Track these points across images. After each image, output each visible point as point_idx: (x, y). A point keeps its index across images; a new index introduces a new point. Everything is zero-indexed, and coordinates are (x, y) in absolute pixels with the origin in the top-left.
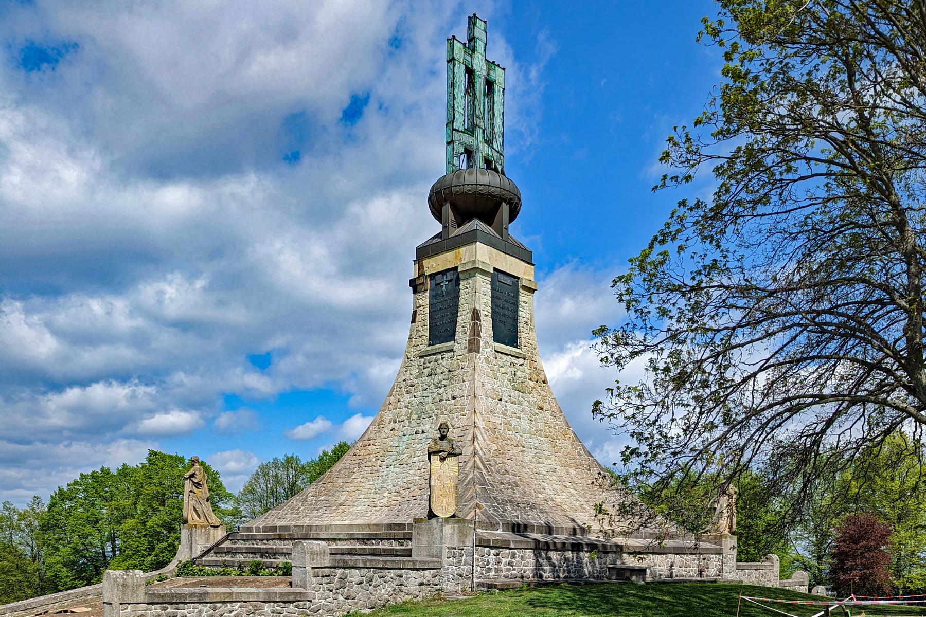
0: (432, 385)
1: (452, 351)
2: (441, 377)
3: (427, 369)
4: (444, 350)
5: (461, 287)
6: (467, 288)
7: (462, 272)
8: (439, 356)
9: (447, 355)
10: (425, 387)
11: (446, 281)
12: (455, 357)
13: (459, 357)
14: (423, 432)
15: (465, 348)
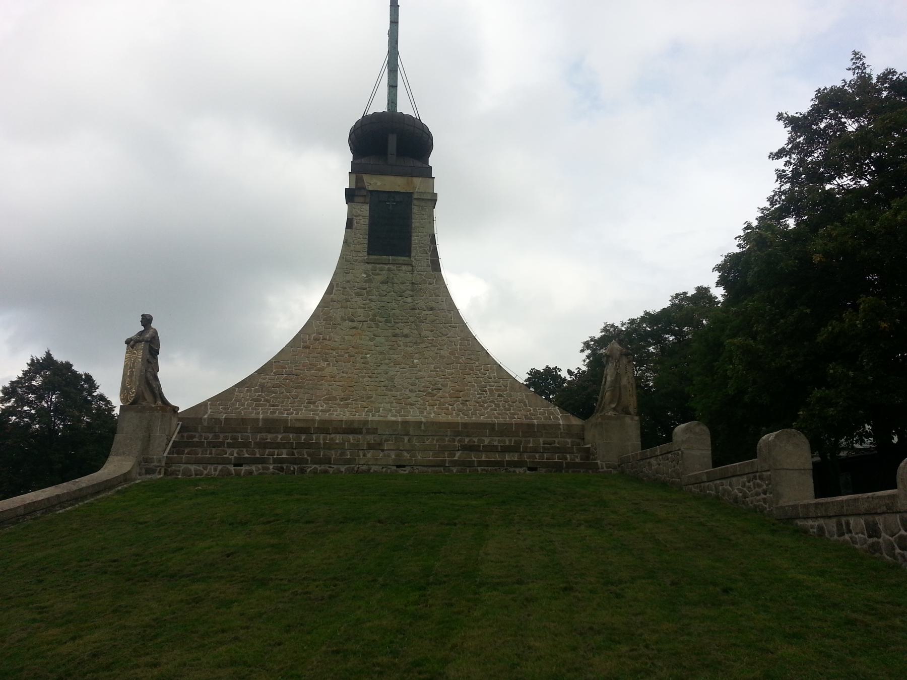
0: (393, 293)
1: (411, 265)
2: (402, 287)
3: (378, 276)
4: (400, 262)
5: (414, 211)
6: (423, 215)
7: (418, 199)
8: (392, 267)
9: (404, 268)
10: (384, 293)
11: (394, 202)
12: (416, 272)
13: (422, 273)
14: (406, 336)
15: (428, 266)
